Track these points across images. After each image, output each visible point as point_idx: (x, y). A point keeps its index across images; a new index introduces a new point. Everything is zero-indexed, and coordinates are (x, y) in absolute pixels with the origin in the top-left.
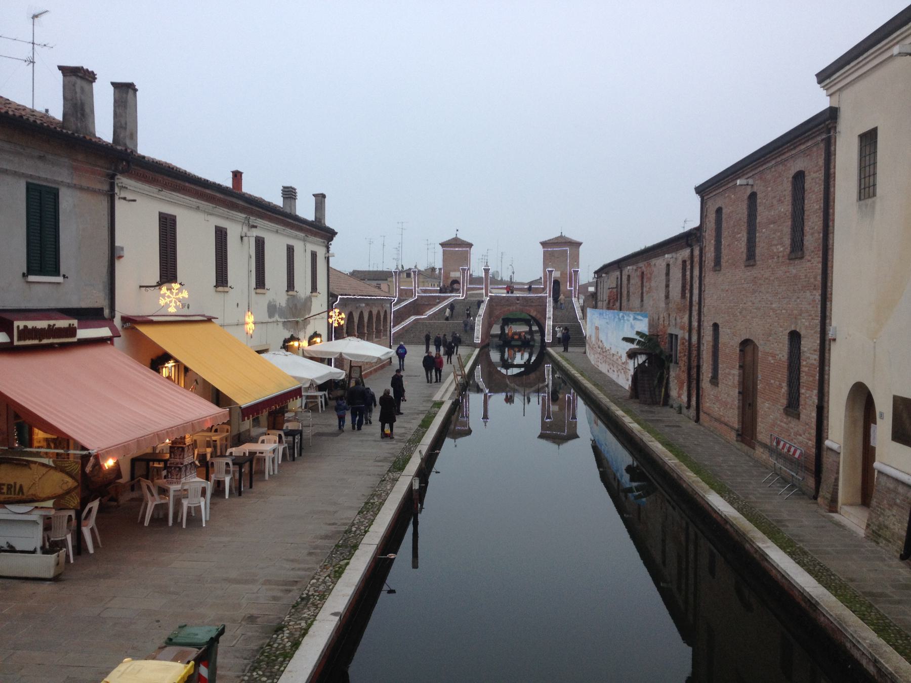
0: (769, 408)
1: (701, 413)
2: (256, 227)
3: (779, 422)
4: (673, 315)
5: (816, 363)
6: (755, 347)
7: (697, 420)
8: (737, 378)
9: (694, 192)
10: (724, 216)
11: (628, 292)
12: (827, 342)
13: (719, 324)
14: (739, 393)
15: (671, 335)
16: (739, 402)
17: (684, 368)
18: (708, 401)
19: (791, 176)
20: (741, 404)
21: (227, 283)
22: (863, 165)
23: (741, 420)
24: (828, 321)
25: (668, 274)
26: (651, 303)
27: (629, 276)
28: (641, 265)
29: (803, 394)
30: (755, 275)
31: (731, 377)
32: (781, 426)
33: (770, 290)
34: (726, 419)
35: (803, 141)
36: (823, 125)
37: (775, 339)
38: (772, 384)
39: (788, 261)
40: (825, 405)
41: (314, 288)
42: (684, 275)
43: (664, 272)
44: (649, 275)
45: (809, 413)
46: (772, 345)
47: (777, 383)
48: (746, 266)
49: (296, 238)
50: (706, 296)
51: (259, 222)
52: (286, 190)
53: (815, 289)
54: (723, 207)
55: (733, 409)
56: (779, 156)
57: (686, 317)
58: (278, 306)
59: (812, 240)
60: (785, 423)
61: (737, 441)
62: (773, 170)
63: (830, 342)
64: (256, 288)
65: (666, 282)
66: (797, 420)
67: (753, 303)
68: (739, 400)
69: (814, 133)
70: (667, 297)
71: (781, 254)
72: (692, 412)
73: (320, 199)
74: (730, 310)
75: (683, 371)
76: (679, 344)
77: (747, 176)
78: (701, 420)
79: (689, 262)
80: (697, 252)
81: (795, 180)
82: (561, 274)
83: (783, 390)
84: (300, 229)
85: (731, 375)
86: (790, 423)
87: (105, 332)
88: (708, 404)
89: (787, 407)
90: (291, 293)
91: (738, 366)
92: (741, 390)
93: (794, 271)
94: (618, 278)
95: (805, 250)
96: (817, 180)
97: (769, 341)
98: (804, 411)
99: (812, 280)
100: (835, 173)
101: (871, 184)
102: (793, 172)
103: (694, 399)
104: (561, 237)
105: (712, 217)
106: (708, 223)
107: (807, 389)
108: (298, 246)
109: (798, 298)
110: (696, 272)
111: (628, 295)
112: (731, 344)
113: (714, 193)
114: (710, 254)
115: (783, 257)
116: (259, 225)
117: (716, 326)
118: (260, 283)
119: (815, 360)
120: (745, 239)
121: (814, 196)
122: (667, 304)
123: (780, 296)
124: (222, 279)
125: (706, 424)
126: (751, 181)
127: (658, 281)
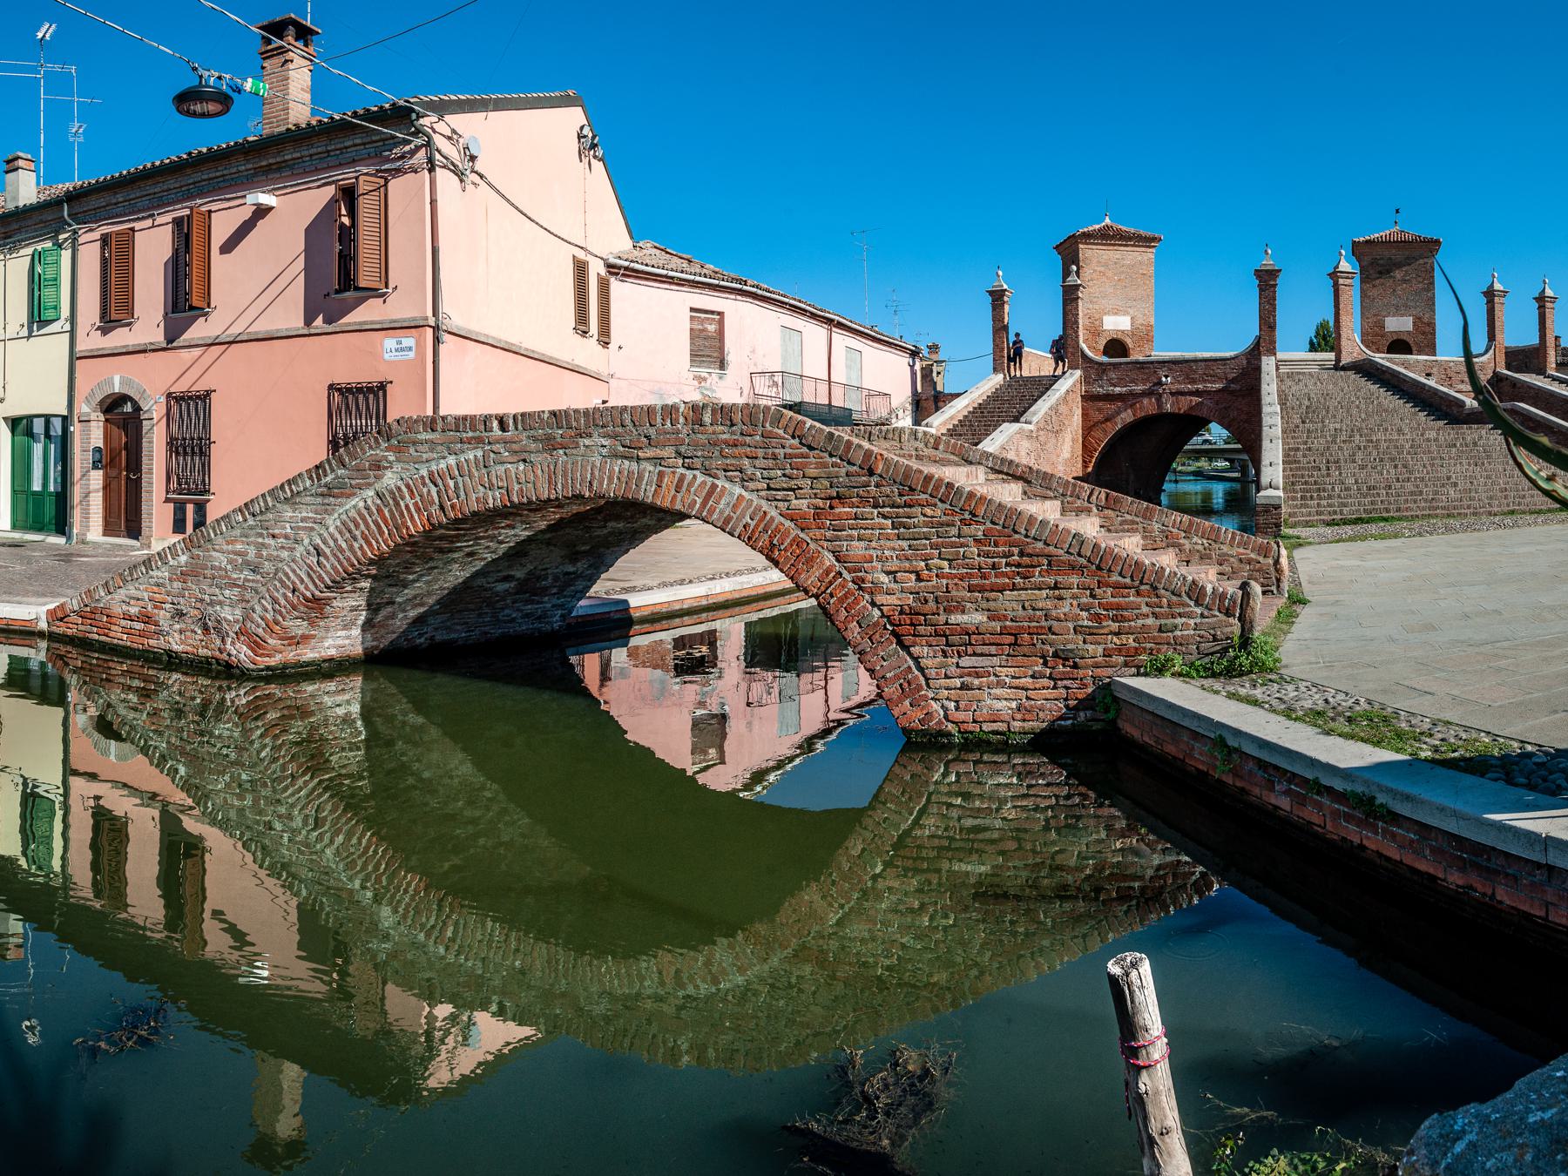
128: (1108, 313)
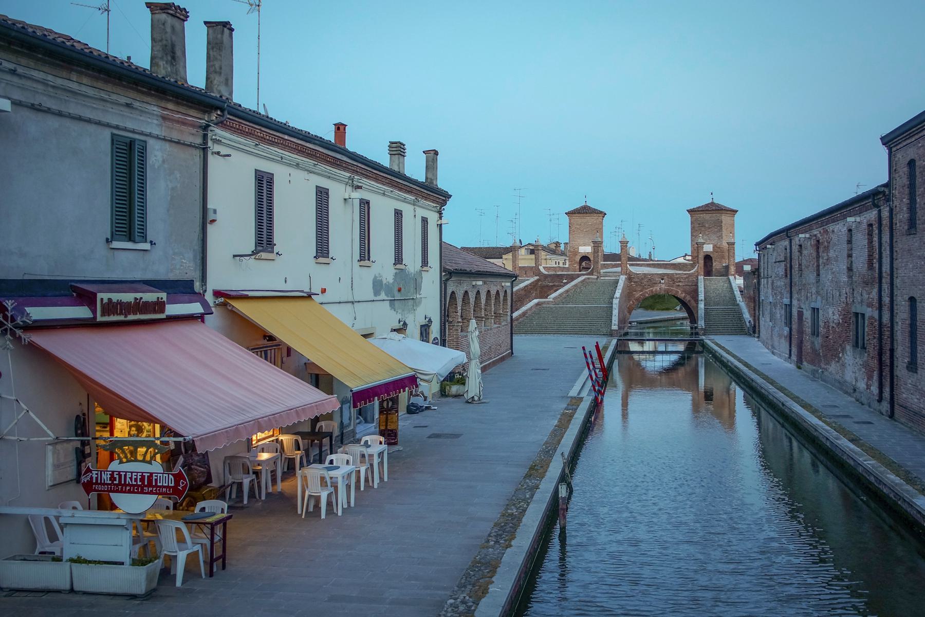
1: (896, 407)
2: (360, 187)
7: (892, 416)
13: (917, 298)
15: (856, 314)
18: (903, 390)
21: (328, 253)
25: (850, 242)
26: (830, 277)
27: (800, 246)
28: (815, 232)
41: (425, 262)
42: (870, 242)
44: (826, 244)
49: (405, 201)
51: (365, 182)
52: (394, 145)
54: (917, 159)
57: (875, 290)
58: (384, 282)
65: (848, 250)
70: (850, 269)
72: (885, 406)
73: (432, 156)
76: (866, 325)
79: (877, 225)
84: (410, 191)
87: (195, 308)
88: (904, 395)
90: (398, 266)
94: (786, 249)
103: (887, 390)
104: (712, 204)
105: (904, 170)
106: (898, 179)
108: (407, 210)
110: (886, 238)
111: (801, 270)
113: (904, 144)
116: (364, 186)
118: (365, 254)
122: (850, 277)
127: (838, 251)
128: (580, 246)
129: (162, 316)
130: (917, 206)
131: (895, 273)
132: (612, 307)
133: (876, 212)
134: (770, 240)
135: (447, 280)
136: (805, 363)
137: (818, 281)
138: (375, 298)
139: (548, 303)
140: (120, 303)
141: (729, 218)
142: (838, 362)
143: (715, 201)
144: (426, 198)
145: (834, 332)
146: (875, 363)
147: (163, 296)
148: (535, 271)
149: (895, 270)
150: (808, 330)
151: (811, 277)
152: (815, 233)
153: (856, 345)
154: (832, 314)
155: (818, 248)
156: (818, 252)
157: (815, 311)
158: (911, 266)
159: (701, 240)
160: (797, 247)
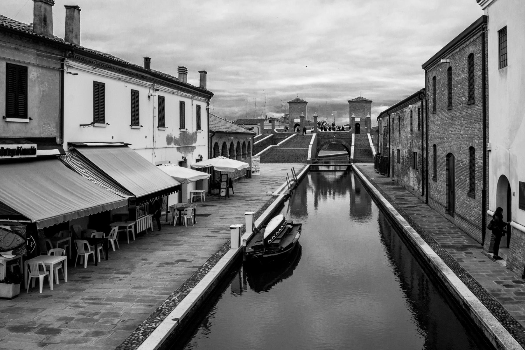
0: (460, 193)
1: (429, 198)
3: (465, 201)
4: (415, 141)
5: (482, 165)
6: (454, 157)
7: (427, 203)
8: (445, 176)
9: (422, 68)
10: (437, 81)
11: (393, 128)
12: (487, 152)
14: (447, 185)
15: (414, 153)
16: (447, 191)
17: (420, 172)
18: (432, 190)
19: (467, 57)
20: (448, 192)
22: (501, 49)
23: (448, 201)
24: (487, 140)
25: (411, 117)
26: (404, 134)
27: (393, 119)
28: (399, 112)
29: (476, 184)
30: (452, 115)
31: (442, 176)
32: (467, 204)
33: (459, 124)
34: (441, 201)
35: (472, 36)
36: (480, 26)
37: (463, 152)
38: (462, 179)
39: (467, 106)
40: (487, 189)
43: (410, 115)
44: (403, 118)
45: (479, 195)
46: (461, 156)
47: (464, 178)
48: (448, 110)
50: (430, 128)
53: (480, 122)
54: (436, 76)
55: (444, 195)
56: (461, 45)
57: (421, 141)
59: (478, 92)
60: (469, 202)
61: (446, 213)
62: (458, 53)
63: (488, 152)
64: (159, 127)
66: (474, 200)
67: (452, 132)
68: (446, 189)
69: (477, 31)
70: (411, 130)
71: (464, 102)
74: (441, 136)
75: (420, 174)
77: (446, 58)
78: (429, 203)
80: (424, 103)
81: (469, 59)
82: (360, 119)
83: (467, 182)
85: (443, 174)
86: (471, 201)
87: (56, 152)
89: (469, 192)
91: (446, 169)
92: (448, 183)
93: (470, 111)
95: (475, 98)
96: (479, 58)
97: (460, 153)
98: (477, 194)
99: (479, 116)
100: (487, 54)
101: (505, 59)
102: (468, 54)
103: (425, 190)
104: (360, 98)
105: (431, 81)
107: (478, 181)
109: (473, 127)
110: (425, 115)
111: (393, 130)
112: (442, 156)
114: (431, 104)
115: (465, 103)
117: (435, 146)
118: (162, 123)
119: (482, 163)
120: (447, 94)
121: (478, 67)
122: (412, 134)
123: (464, 126)
124: (135, 121)
125: (431, 205)
126: (448, 61)
129: (35, 156)
130: (437, 99)
131: (428, 132)
132: (308, 149)
133: (421, 102)
134: (382, 116)
135: (212, 136)
136: (395, 177)
137: (400, 136)
138: (168, 146)
139: (277, 147)
140: (8, 149)
141: (368, 105)
142: (407, 176)
143: (362, 96)
144: (199, 95)
145: (406, 161)
146: (420, 177)
147: (35, 146)
148: (272, 131)
149: (428, 131)
150: (396, 160)
151: (397, 134)
152: (399, 112)
153: (414, 168)
154: (405, 153)
155: (400, 120)
156: (400, 122)
157: (399, 151)
158: (434, 129)
159: (353, 116)
160: (392, 119)
